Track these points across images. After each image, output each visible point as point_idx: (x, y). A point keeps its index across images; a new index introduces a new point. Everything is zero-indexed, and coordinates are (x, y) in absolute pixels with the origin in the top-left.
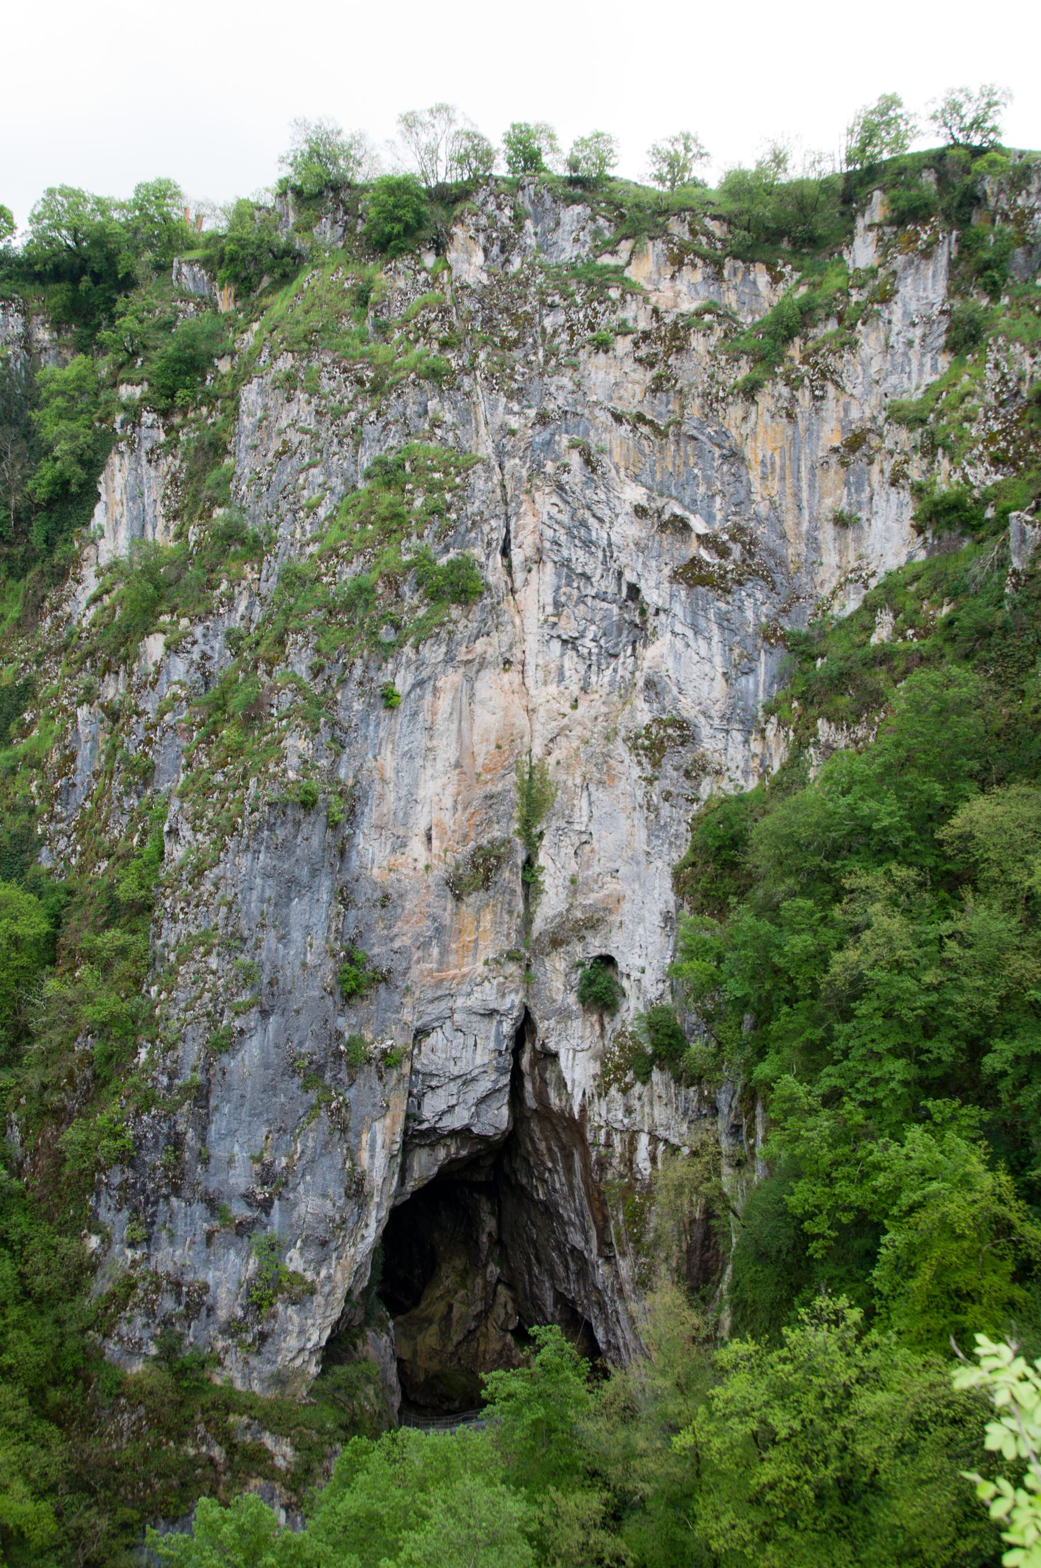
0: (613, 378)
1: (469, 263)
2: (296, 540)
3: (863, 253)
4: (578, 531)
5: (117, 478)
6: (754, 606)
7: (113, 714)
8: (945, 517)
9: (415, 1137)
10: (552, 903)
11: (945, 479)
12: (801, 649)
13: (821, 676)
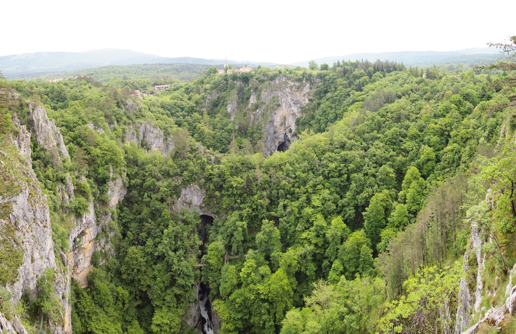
0: (288, 90)
1: (277, 82)
2: (267, 103)
3: (304, 82)
4: (286, 100)
5: (252, 97)
6: (299, 105)
7: (254, 115)
8: (310, 100)
9: (279, 142)
10: (287, 125)
11: (310, 98)
12: (302, 108)
13: (303, 110)
